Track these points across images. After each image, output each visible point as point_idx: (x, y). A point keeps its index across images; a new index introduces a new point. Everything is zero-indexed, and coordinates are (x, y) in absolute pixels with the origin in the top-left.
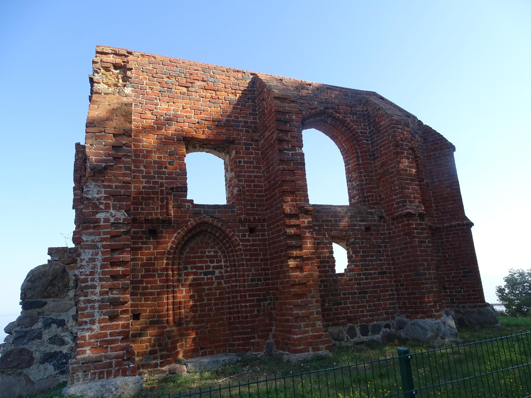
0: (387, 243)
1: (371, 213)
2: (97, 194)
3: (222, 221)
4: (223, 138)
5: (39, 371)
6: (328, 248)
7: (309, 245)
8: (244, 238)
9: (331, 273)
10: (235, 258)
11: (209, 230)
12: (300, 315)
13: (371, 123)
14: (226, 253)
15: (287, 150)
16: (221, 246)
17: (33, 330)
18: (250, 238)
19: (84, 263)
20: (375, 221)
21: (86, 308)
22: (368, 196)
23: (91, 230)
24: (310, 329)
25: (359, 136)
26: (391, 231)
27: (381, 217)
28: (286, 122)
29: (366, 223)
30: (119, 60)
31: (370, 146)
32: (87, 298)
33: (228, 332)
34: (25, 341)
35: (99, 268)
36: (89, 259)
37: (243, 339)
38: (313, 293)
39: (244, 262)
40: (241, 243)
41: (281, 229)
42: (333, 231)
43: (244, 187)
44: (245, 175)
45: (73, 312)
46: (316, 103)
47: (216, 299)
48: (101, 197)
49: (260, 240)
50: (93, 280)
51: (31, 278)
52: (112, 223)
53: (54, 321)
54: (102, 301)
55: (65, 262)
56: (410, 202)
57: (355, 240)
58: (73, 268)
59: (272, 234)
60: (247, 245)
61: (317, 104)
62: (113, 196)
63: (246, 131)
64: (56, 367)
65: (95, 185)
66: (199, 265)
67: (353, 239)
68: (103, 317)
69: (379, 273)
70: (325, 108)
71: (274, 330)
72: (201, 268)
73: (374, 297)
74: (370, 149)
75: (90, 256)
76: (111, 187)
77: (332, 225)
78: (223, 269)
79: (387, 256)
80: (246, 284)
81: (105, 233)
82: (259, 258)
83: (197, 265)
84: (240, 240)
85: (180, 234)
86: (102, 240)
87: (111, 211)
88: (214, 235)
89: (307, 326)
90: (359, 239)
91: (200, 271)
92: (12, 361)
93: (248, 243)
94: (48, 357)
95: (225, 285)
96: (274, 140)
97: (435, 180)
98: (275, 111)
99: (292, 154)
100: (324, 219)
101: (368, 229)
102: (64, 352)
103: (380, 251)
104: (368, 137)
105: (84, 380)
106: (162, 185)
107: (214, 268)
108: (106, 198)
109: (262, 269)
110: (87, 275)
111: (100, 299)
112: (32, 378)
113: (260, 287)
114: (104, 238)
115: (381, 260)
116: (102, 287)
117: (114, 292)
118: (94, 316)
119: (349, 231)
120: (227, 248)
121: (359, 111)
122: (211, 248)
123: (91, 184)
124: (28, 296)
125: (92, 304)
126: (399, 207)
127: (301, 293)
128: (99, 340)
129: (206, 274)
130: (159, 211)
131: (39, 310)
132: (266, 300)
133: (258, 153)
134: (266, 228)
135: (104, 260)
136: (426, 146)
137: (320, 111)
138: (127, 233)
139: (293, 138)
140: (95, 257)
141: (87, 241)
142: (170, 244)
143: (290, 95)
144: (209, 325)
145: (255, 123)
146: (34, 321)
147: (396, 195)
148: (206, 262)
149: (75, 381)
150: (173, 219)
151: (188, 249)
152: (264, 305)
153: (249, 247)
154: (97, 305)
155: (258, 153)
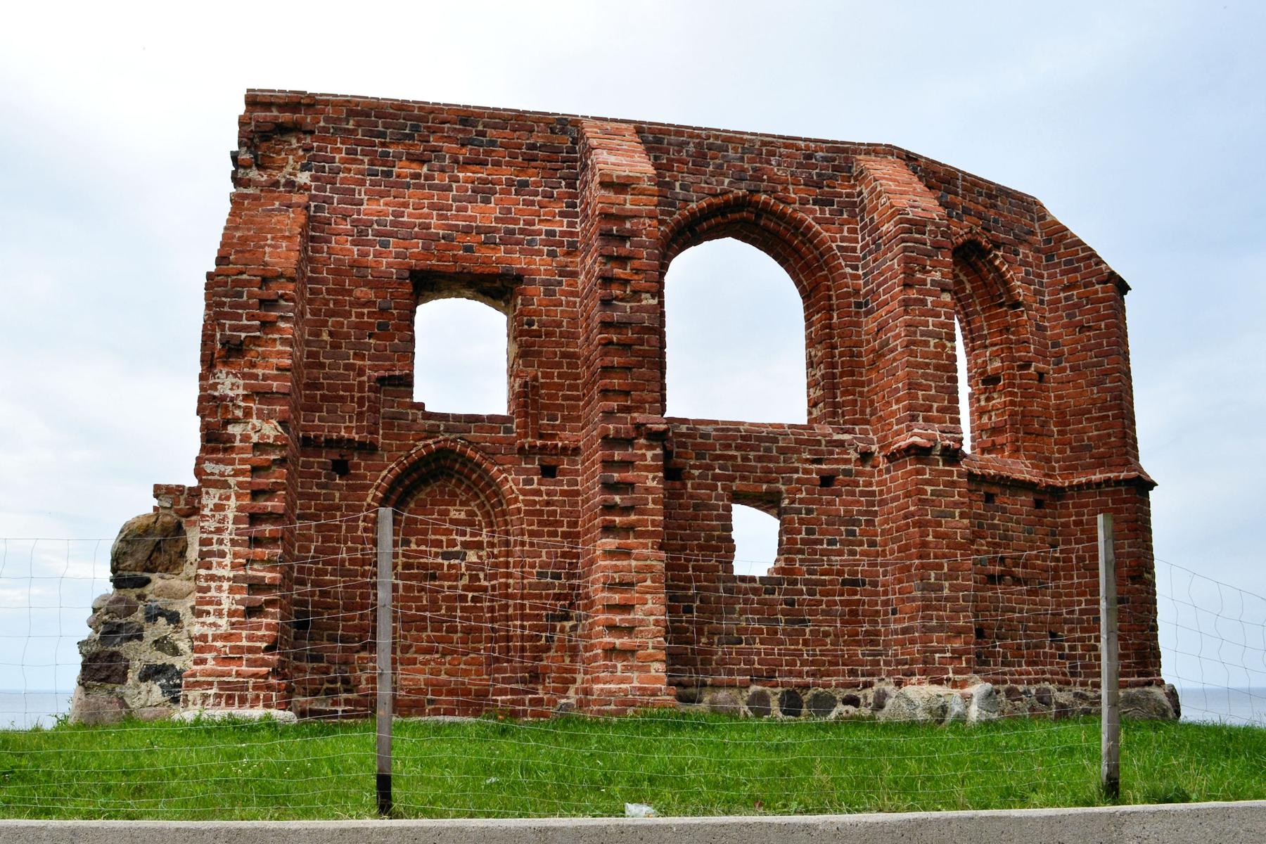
0: (875, 514)
1: (841, 444)
2: (231, 389)
3: (484, 449)
4: (496, 270)
5: (139, 693)
6: (719, 517)
7: (651, 506)
8: (528, 487)
9: (721, 573)
10: (509, 527)
11: (457, 466)
12: (617, 646)
14: (493, 518)
15: (622, 300)
16: (483, 502)
17: (130, 623)
18: (543, 488)
20: (848, 461)
21: (208, 589)
22: (844, 404)
23: (220, 455)
24: (635, 675)
25: (835, 257)
26: (884, 488)
27: (866, 456)
28: (622, 238)
29: (824, 466)
30: (286, 117)
31: (861, 282)
32: (210, 572)
33: (485, 677)
34: (119, 639)
35: (231, 522)
36: (215, 505)
37: (513, 692)
38: (650, 605)
40: (521, 497)
42: (738, 482)
43: (535, 378)
44: (542, 352)
45: (191, 602)
46: (727, 181)
47: (463, 609)
48: (238, 395)
49: (563, 493)
50: (220, 542)
51: (126, 535)
53: (162, 613)
54: (235, 579)
55: (182, 513)
56: (926, 419)
57: (793, 502)
58: (194, 523)
59: (587, 480)
60: (535, 503)
61: (730, 183)
62: (258, 393)
63: (552, 254)
64: (166, 689)
65: (228, 374)
66: (433, 537)
67: (787, 501)
68: (234, 607)
69: (844, 583)
70: (751, 192)
71: (579, 681)
72: (438, 544)
73: (826, 634)
74: (860, 290)
75: (216, 501)
76: (255, 377)
77: (736, 468)
78: (483, 549)
79: (872, 544)
80: (525, 581)
81: (243, 461)
82: (560, 530)
83: (429, 537)
84: (518, 490)
85: (393, 472)
86: (237, 473)
87: (254, 421)
88: (469, 479)
89: (626, 669)
90: (801, 501)
91: (436, 550)
92: (98, 670)
93: (537, 498)
94: (151, 673)
95: (486, 583)
97: (1063, 364)
98: (600, 214)
99: (631, 308)
100: (718, 452)
101: (827, 480)
102: (178, 668)
103: (853, 533)
104: (858, 259)
105: (203, 703)
106: (361, 372)
107: (466, 545)
108: (246, 398)
109: (564, 555)
110: (211, 532)
111: (231, 575)
112: (128, 701)
113: (556, 591)
114: (240, 470)
115: (853, 553)
116: (235, 555)
117: (255, 566)
118: (221, 604)
119: (778, 482)
120: (493, 506)
121: (840, 195)
122: (460, 505)
123: (221, 372)
124: (121, 566)
125: (218, 583)
127: (623, 602)
128: (229, 644)
129: (446, 556)
130: (354, 424)
131: (138, 591)
132: (567, 617)
133: (575, 303)
134: (579, 467)
135: (240, 509)
136: (1050, 276)
137: (736, 198)
138: (282, 462)
139: (636, 273)
140: (225, 502)
141: (212, 474)
142: (372, 491)
143: (638, 175)
144: (449, 658)
145: (572, 234)
146: (131, 610)
147: (898, 401)
148: (448, 532)
149: (190, 703)
150: (381, 441)
151: (412, 505)
152: (562, 630)
153: (538, 507)
154: (226, 585)
155: (575, 303)
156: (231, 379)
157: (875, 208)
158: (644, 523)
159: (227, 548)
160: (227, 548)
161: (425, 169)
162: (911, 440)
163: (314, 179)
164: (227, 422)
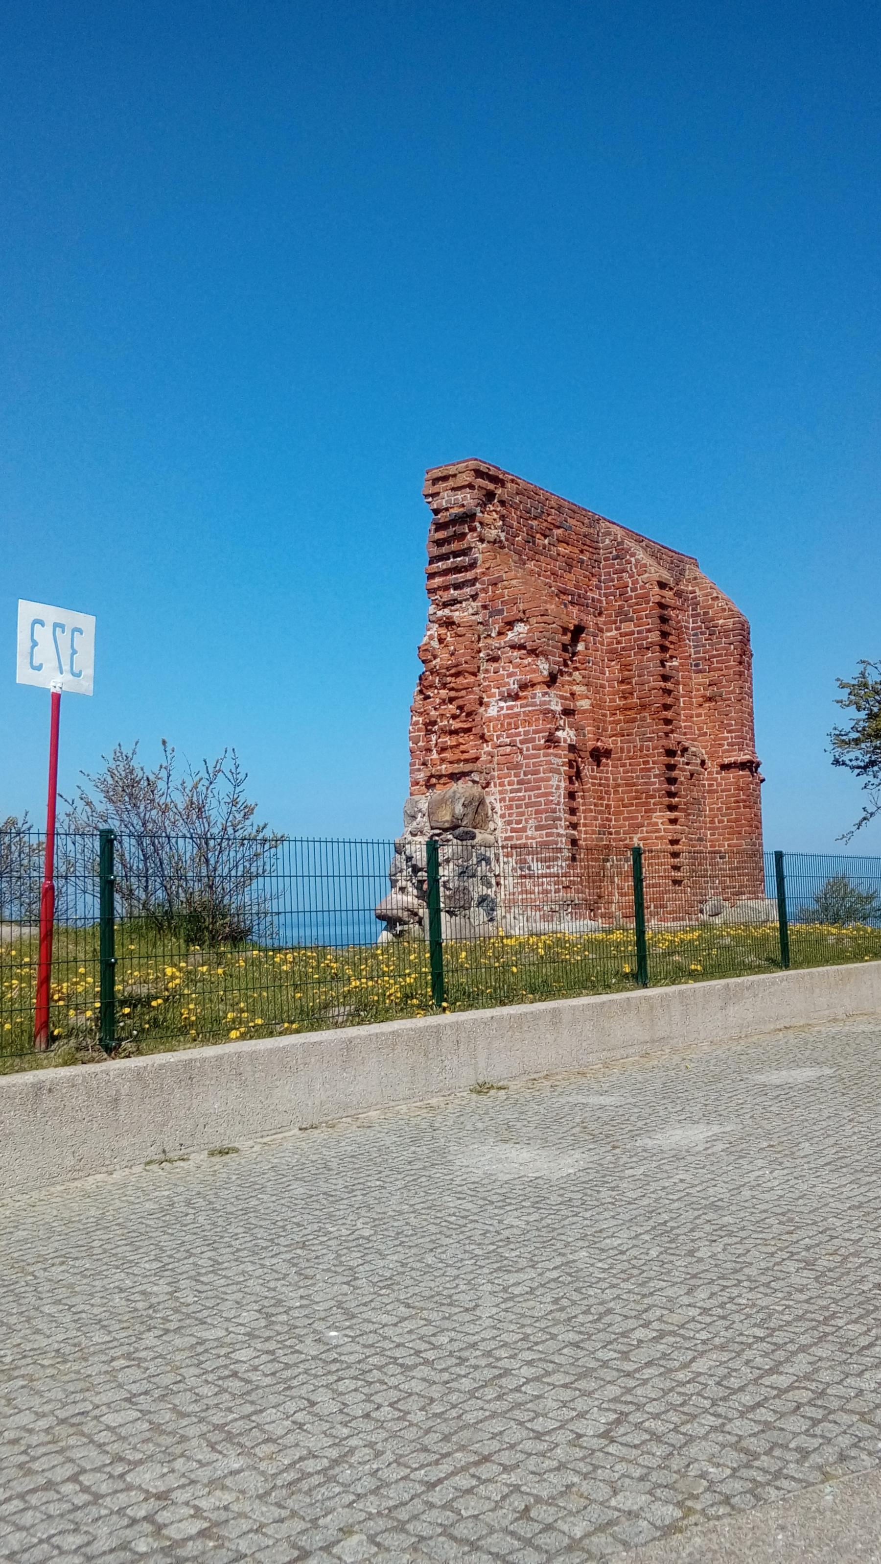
13: (698, 615)
19: (554, 791)
23: (551, 751)
39: (592, 807)
41: (654, 768)
52: (570, 745)
54: (566, 836)
58: (488, 793)
64: (488, 914)
87: (567, 729)
94: (483, 900)
96: (651, 643)
101: (692, 775)
126: (734, 750)
147: (729, 732)
154: (564, 839)
156: (555, 699)
157: (711, 607)
158: (679, 803)
159: (562, 815)
160: (562, 815)
161: (546, 541)
162: (745, 757)
163: (507, 540)
164: (557, 729)
